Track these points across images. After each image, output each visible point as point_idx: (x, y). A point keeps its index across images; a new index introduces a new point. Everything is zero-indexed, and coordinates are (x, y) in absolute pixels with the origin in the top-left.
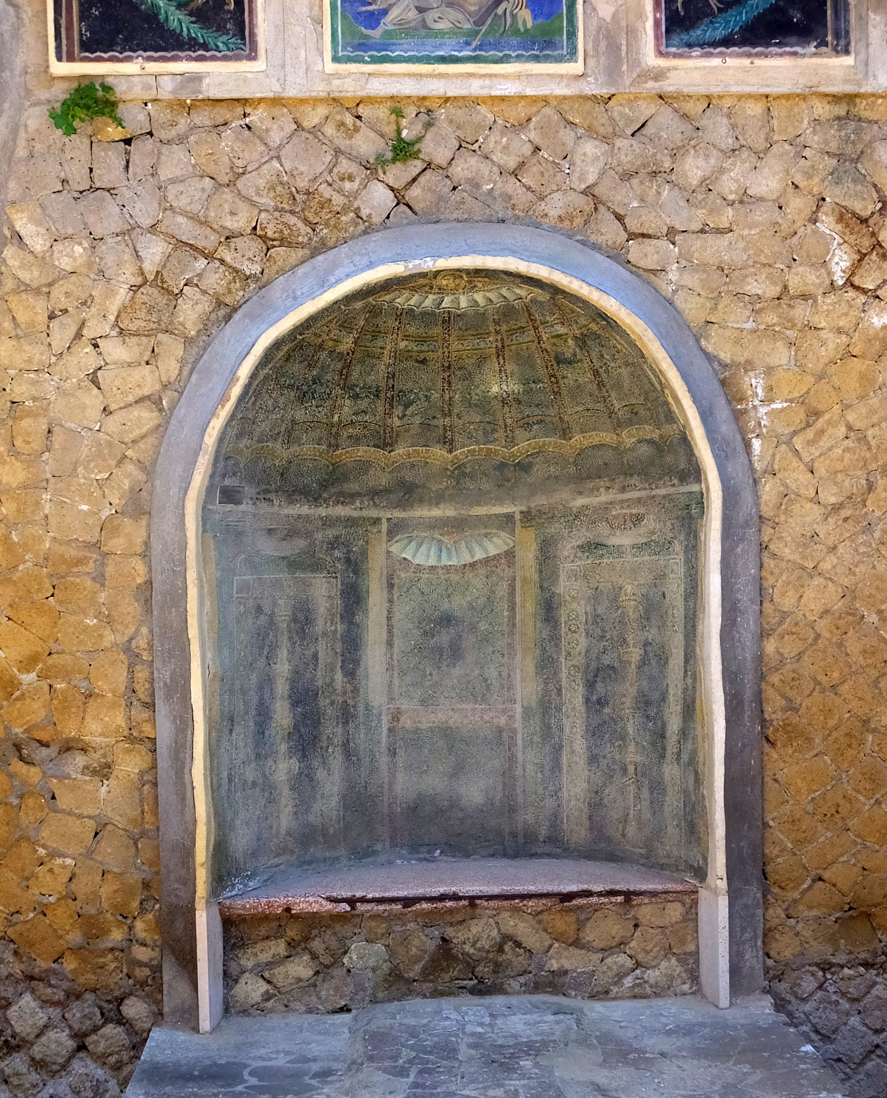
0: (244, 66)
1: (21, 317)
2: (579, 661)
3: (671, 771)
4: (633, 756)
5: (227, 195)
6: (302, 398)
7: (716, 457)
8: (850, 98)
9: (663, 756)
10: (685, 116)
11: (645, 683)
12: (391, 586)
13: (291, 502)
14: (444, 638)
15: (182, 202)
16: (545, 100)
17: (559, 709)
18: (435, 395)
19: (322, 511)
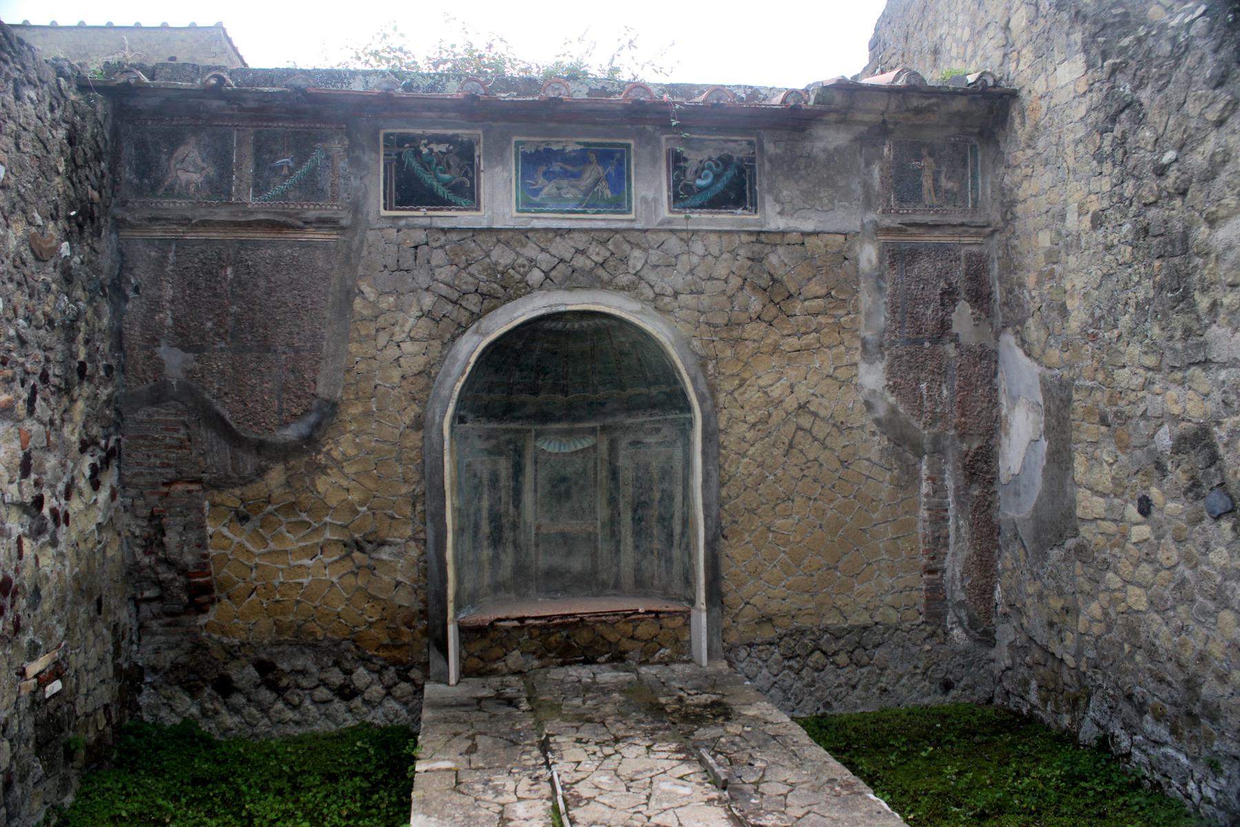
0: (475, 213)
1: (363, 332)
2: (629, 499)
3: (676, 553)
4: (656, 545)
5: (464, 274)
6: (496, 372)
7: (699, 401)
8: (759, 233)
9: (672, 545)
10: (682, 239)
11: (662, 510)
12: (536, 463)
13: (489, 422)
14: (562, 488)
15: (442, 277)
16: (616, 231)
17: (619, 523)
18: (559, 369)
19: (504, 426)
